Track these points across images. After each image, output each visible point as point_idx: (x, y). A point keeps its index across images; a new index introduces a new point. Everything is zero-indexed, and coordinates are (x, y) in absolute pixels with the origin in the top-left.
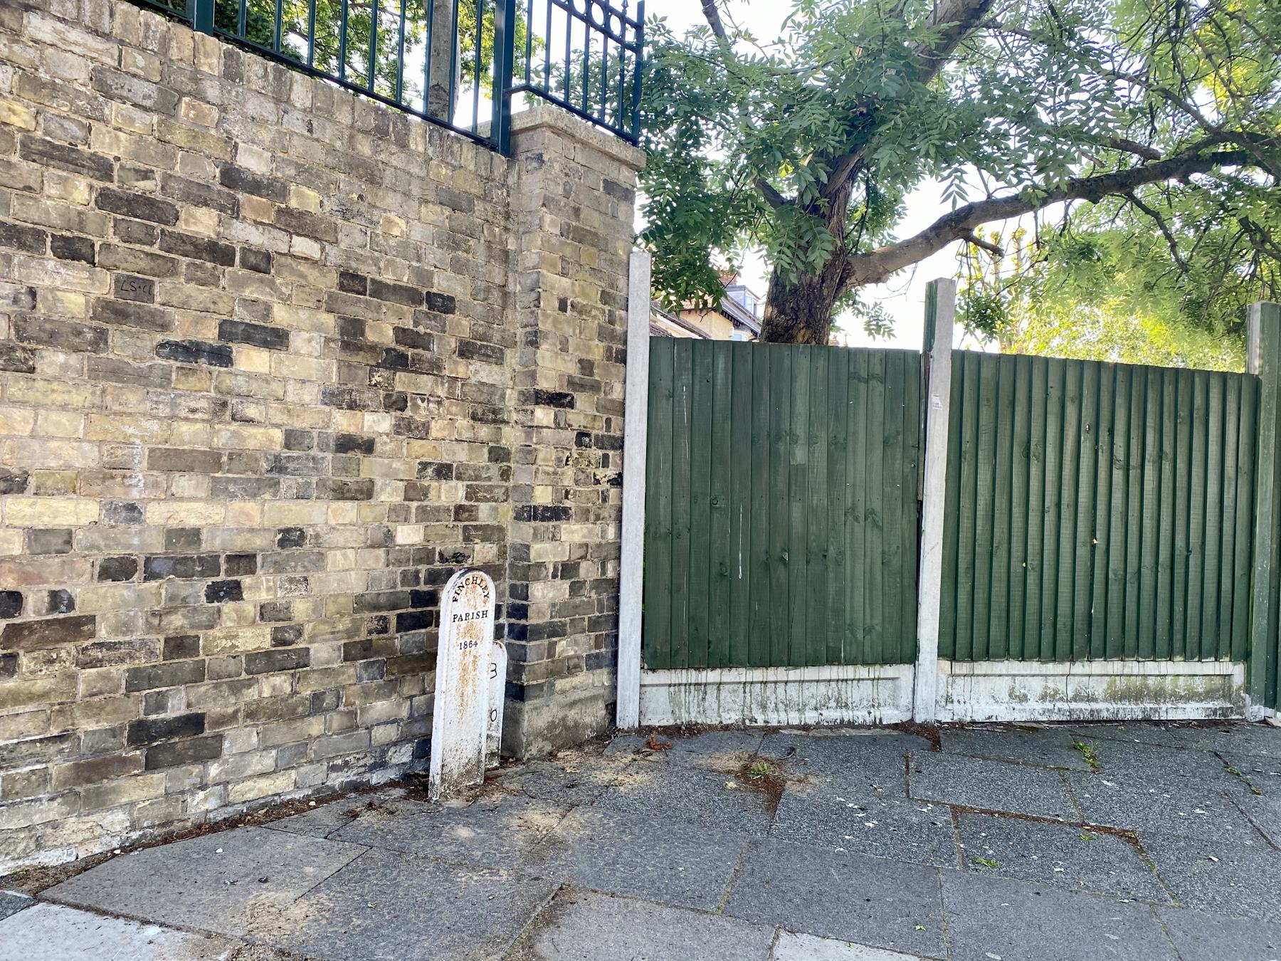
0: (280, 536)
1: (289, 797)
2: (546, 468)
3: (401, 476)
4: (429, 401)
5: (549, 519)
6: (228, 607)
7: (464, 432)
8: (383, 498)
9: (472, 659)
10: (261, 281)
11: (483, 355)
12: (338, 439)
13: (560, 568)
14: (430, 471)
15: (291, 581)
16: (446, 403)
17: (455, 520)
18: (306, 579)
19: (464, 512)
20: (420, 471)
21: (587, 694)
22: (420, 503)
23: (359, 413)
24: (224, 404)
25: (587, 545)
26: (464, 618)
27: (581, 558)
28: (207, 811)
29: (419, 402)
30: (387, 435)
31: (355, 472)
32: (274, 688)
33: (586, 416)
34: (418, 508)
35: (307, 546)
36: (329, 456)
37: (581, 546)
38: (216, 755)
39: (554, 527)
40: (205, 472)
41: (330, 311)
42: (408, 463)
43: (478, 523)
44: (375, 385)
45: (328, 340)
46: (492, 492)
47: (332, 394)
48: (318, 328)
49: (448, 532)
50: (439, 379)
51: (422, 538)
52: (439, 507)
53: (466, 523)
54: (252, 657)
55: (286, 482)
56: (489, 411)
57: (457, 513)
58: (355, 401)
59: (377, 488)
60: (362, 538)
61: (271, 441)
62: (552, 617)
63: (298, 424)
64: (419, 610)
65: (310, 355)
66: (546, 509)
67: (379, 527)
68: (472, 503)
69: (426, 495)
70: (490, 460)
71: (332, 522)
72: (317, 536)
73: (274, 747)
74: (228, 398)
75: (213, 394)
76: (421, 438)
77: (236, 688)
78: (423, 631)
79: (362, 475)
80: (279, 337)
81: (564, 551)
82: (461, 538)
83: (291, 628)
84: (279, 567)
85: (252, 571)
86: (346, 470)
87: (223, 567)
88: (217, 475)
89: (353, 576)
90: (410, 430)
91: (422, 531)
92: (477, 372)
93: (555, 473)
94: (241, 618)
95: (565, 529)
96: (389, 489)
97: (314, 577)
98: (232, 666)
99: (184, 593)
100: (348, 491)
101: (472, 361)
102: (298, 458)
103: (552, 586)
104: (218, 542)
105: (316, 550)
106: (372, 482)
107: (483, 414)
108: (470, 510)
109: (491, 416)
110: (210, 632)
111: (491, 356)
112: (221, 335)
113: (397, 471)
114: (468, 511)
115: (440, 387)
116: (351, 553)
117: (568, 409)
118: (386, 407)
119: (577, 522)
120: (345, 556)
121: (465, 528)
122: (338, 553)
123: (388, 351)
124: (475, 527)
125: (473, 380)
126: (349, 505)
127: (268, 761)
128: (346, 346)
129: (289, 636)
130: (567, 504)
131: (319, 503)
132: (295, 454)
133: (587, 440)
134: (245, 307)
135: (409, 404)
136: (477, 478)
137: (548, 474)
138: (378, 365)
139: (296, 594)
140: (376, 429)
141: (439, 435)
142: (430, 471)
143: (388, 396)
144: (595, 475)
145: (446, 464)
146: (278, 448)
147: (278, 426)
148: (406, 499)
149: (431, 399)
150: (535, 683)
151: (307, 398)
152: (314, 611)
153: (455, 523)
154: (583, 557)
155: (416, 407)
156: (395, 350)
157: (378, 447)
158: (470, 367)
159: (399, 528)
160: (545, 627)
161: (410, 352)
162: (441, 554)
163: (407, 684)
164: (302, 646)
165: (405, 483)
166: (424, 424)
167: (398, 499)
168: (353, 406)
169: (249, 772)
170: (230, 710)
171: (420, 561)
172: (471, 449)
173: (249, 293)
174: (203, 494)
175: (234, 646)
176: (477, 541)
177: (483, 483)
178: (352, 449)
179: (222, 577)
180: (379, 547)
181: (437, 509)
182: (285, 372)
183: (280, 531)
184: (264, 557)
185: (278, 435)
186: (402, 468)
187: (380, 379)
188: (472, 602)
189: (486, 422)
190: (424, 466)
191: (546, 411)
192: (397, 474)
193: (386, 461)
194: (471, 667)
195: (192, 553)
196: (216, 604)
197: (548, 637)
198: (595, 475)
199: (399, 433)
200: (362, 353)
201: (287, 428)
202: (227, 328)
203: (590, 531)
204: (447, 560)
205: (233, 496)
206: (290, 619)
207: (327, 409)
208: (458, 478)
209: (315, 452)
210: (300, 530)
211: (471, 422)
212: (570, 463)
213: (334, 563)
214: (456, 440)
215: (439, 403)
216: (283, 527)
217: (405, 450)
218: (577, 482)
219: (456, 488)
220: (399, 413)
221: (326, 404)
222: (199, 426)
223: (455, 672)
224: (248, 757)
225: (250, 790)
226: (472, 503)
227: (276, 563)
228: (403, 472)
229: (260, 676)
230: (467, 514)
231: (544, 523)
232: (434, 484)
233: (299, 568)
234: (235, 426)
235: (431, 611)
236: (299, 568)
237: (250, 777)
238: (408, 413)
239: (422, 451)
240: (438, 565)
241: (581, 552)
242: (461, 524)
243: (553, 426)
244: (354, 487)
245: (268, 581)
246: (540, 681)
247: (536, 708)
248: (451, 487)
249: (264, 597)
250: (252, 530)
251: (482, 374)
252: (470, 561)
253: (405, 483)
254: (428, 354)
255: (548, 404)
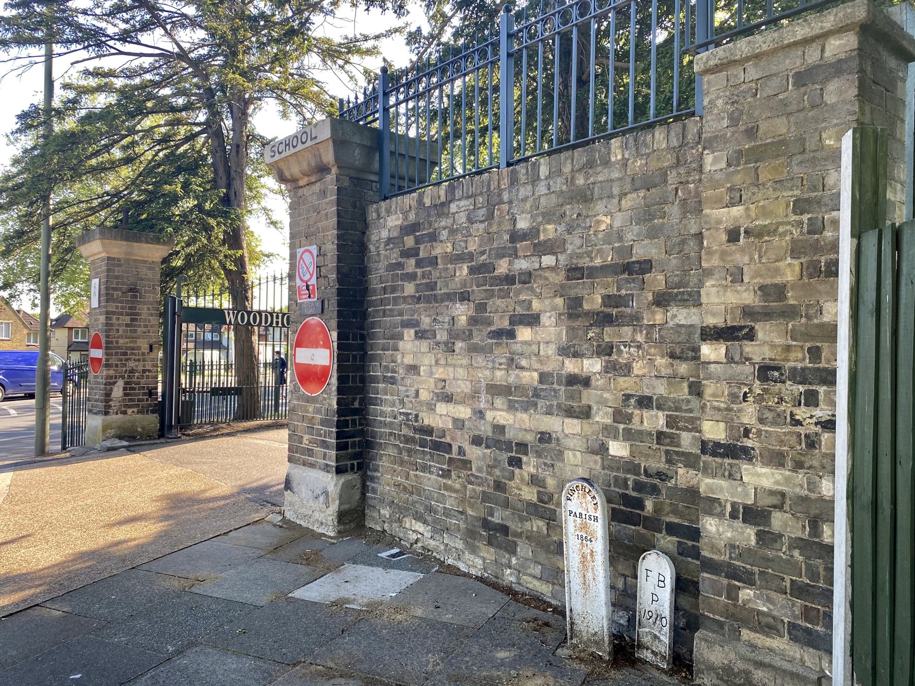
0: (539, 436)
1: (548, 600)
2: (716, 404)
3: (610, 404)
4: (630, 346)
5: (723, 456)
6: (517, 471)
7: (663, 369)
8: (597, 419)
9: (589, 551)
10: (527, 289)
11: (680, 301)
12: (567, 377)
13: (741, 510)
14: (632, 401)
15: (545, 464)
16: (646, 346)
17: (657, 444)
18: (553, 465)
19: (665, 437)
20: (624, 401)
21: (787, 666)
22: (626, 426)
23: (580, 360)
24: (512, 360)
25: (783, 495)
26: (578, 515)
27: (775, 507)
28: (511, 582)
29: (622, 348)
30: (599, 373)
31: (578, 400)
32: (538, 527)
33: (773, 346)
34: (624, 429)
35: (553, 445)
36: (563, 388)
37: (772, 493)
38: (513, 552)
39: (731, 465)
40: (506, 396)
41: (561, 296)
42: (615, 394)
43: (681, 450)
44: (590, 339)
45: (560, 315)
46: (693, 423)
47: (563, 349)
48: (554, 308)
49: (651, 452)
50: (638, 328)
51: (629, 453)
52: (642, 430)
53: (668, 448)
54: (529, 504)
55: (541, 403)
56: (688, 349)
57: (658, 438)
58: (577, 352)
59: (593, 412)
60: (585, 445)
61: (533, 379)
62: (731, 558)
63: (547, 368)
64: (629, 510)
65: (551, 326)
66: (717, 445)
67: (596, 440)
68: (674, 431)
69: (630, 421)
70: (690, 393)
71: (567, 432)
72: (558, 439)
73: (539, 563)
74: (514, 356)
75: (508, 355)
76: (625, 376)
77: (522, 519)
78: (633, 527)
79: (583, 402)
80: (535, 318)
81: (747, 494)
82: (663, 459)
83: (546, 493)
84: (539, 454)
85: (526, 454)
86: (571, 397)
87: (514, 449)
88: (511, 398)
89: (580, 470)
90: (615, 370)
91: (628, 448)
92: (675, 316)
93: (729, 409)
94: (522, 480)
95: (746, 470)
96: (601, 413)
97: (559, 464)
98: (519, 506)
99: (499, 459)
100: (575, 411)
101: (669, 308)
102: (546, 389)
103: (730, 526)
104: (512, 434)
105: (558, 448)
106: (590, 407)
107: (682, 352)
108: (671, 437)
109: (690, 354)
110: (510, 483)
111: (687, 300)
112: (510, 324)
113: (606, 400)
114: (669, 437)
115: (639, 335)
116: (578, 454)
117: (745, 342)
118: (598, 354)
119: (765, 464)
120: (574, 455)
121: (667, 452)
122: (570, 453)
123: (598, 314)
124: (677, 453)
125: (671, 324)
126: (575, 421)
127: (537, 570)
128: (571, 316)
129: (546, 498)
130: (749, 443)
131: (559, 418)
132: (544, 387)
133: (776, 374)
134: (519, 305)
135: (614, 350)
136: (677, 409)
137: (719, 409)
138: (591, 325)
139: (548, 473)
140: (591, 370)
141: (640, 373)
142: (632, 401)
143: (599, 346)
144: (792, 415)
145: (647, 396)
146: (536, 383)
147: (536, 370)
148: (614, 421)
149: (632, 344)
150: (711, 616)
151: (550, 352)
152: (558, 486)
153: (658, 446)
154: (780, 507)
155: (620, 352)
156: (602, 312)
157: (593, 383)
158: (668, 314)
159: (611, 443)
160: (721, 565)
161: (614, 312)
162: (645, 470)
163: (621, 564)
164: (552, 507)
165: (613, 409)
166: (626, 365)
167: (609, 421)
168: (576, 355)
169: (528, 571)
170: (519, 530)
171: (628, 471)
172: (669, 384)
173: (522, 297)
174: (505, 408)
175: (520, 495)
176: (680, 465)
177: (684, 414)
178: (576, 384)
179: (513, 454)
180: (597, 454)
181: (641, 432)
182: (539, 339)
183: (539, 433)
184: (532, 447)
185: (536, 375)
186: (610, 398)
187: (593, 335)
188: (584, 505)
189: (686, 359)
190: (627, 397)
191: (714, 347)
192: (607, 403)
193: (599, 392)
194: (589, 557)
195: (502, 438)
196: (512, 468)
197: (727, 577)
198: (792, 415)
199: (607, 372)
200: (580, 319)
201: (541, 371)
202: (512, 319)
203: (787, 480)
204: (651, 476)
205: (517, 410)
206: (545, 488)
207: (561, 358)
208: (659, 408)
209: (555, 386)
210: (549, 434)
211: (670, 360)
212: (751, 399)
213: (568, 458)
214: (656, 376)
215: (639, 347)
216: (540, 430)
217: (612, 385)
218: (761, 420)
219: (657, 416)
220: (607, 358)
221: (560, 355)
222: (503, 372)
223: (575, 554)
224: (528, 562)
225: (531, 583)
226: (674, 431)
227: (537, 451)
228: (611, 401)
229: (532, 517)
230: (668, 440)
231: (717, 459)
232: (637, 412)
233: (549, 458)
234: (517, 372)
235: (640, 515)
236: (549, 458)
237: (530, 575)
238: (614, 357)
239: (626, 385)
240: (643, 478)
241: (775, 500)
242: (662, 448)
243: (725, 360)
244: (577, 410)
245: (534, 461)
246: (717, 617)
247: (706, 640)
248: (652, 416)
249: (532, 470)
250: (526, 430)
251: (680, 317)
252: (673, 481)
253: (613, 409)
254: (629, 310)
255: (717, 339)
